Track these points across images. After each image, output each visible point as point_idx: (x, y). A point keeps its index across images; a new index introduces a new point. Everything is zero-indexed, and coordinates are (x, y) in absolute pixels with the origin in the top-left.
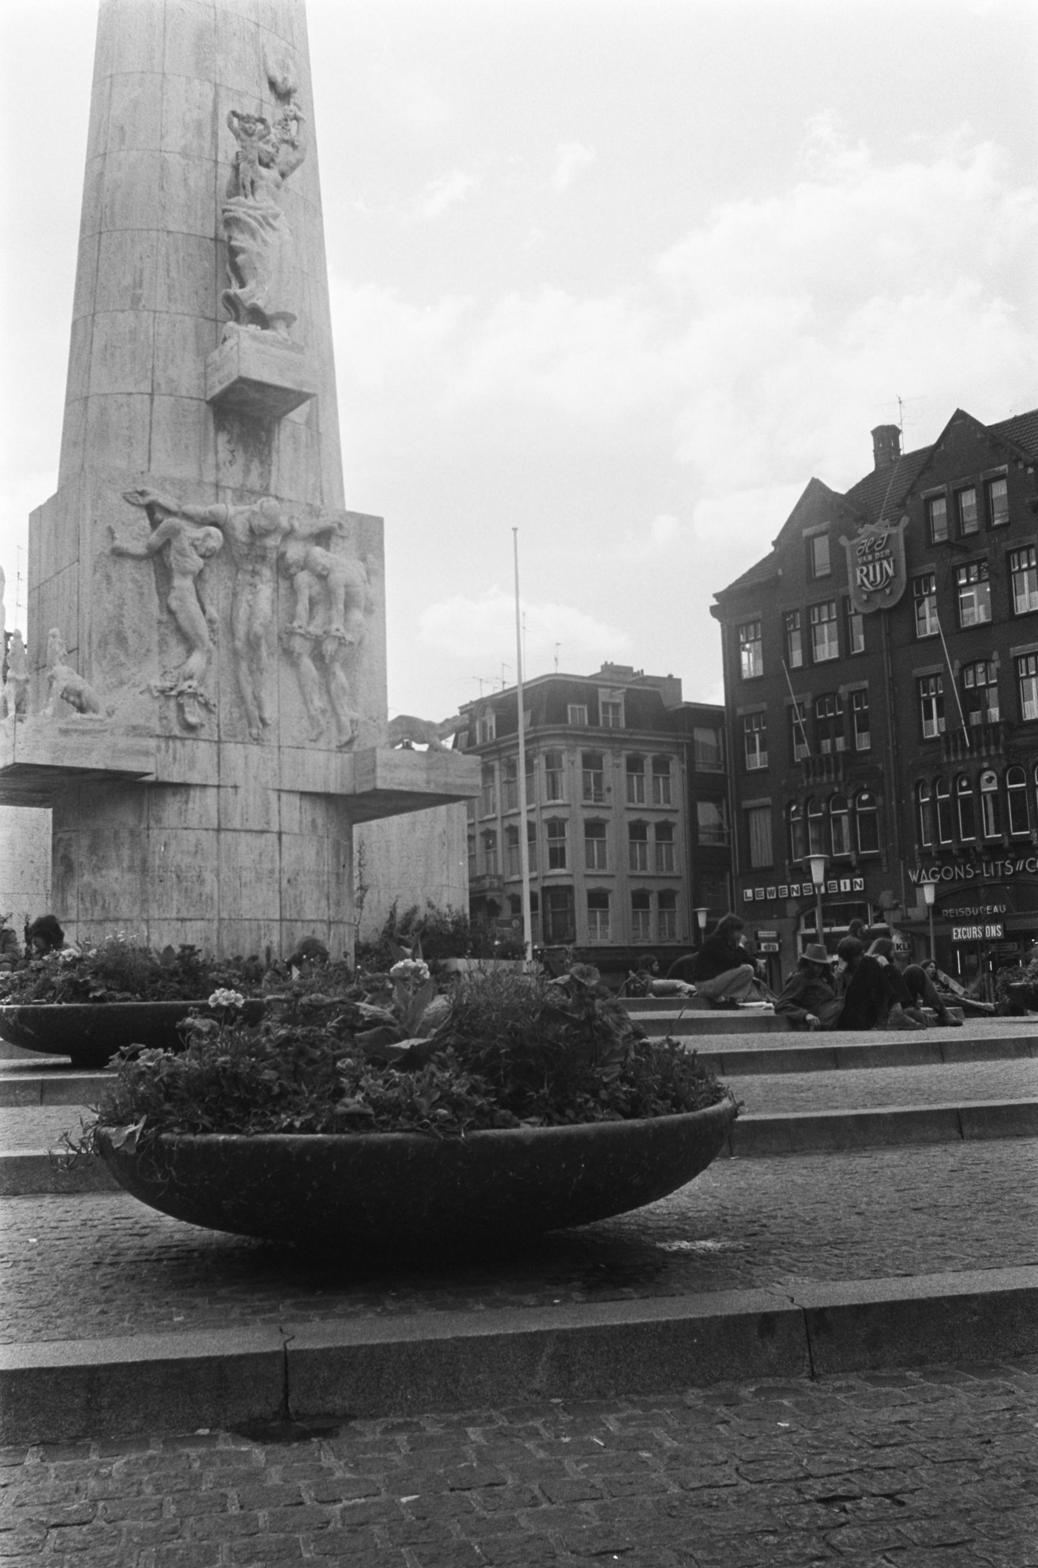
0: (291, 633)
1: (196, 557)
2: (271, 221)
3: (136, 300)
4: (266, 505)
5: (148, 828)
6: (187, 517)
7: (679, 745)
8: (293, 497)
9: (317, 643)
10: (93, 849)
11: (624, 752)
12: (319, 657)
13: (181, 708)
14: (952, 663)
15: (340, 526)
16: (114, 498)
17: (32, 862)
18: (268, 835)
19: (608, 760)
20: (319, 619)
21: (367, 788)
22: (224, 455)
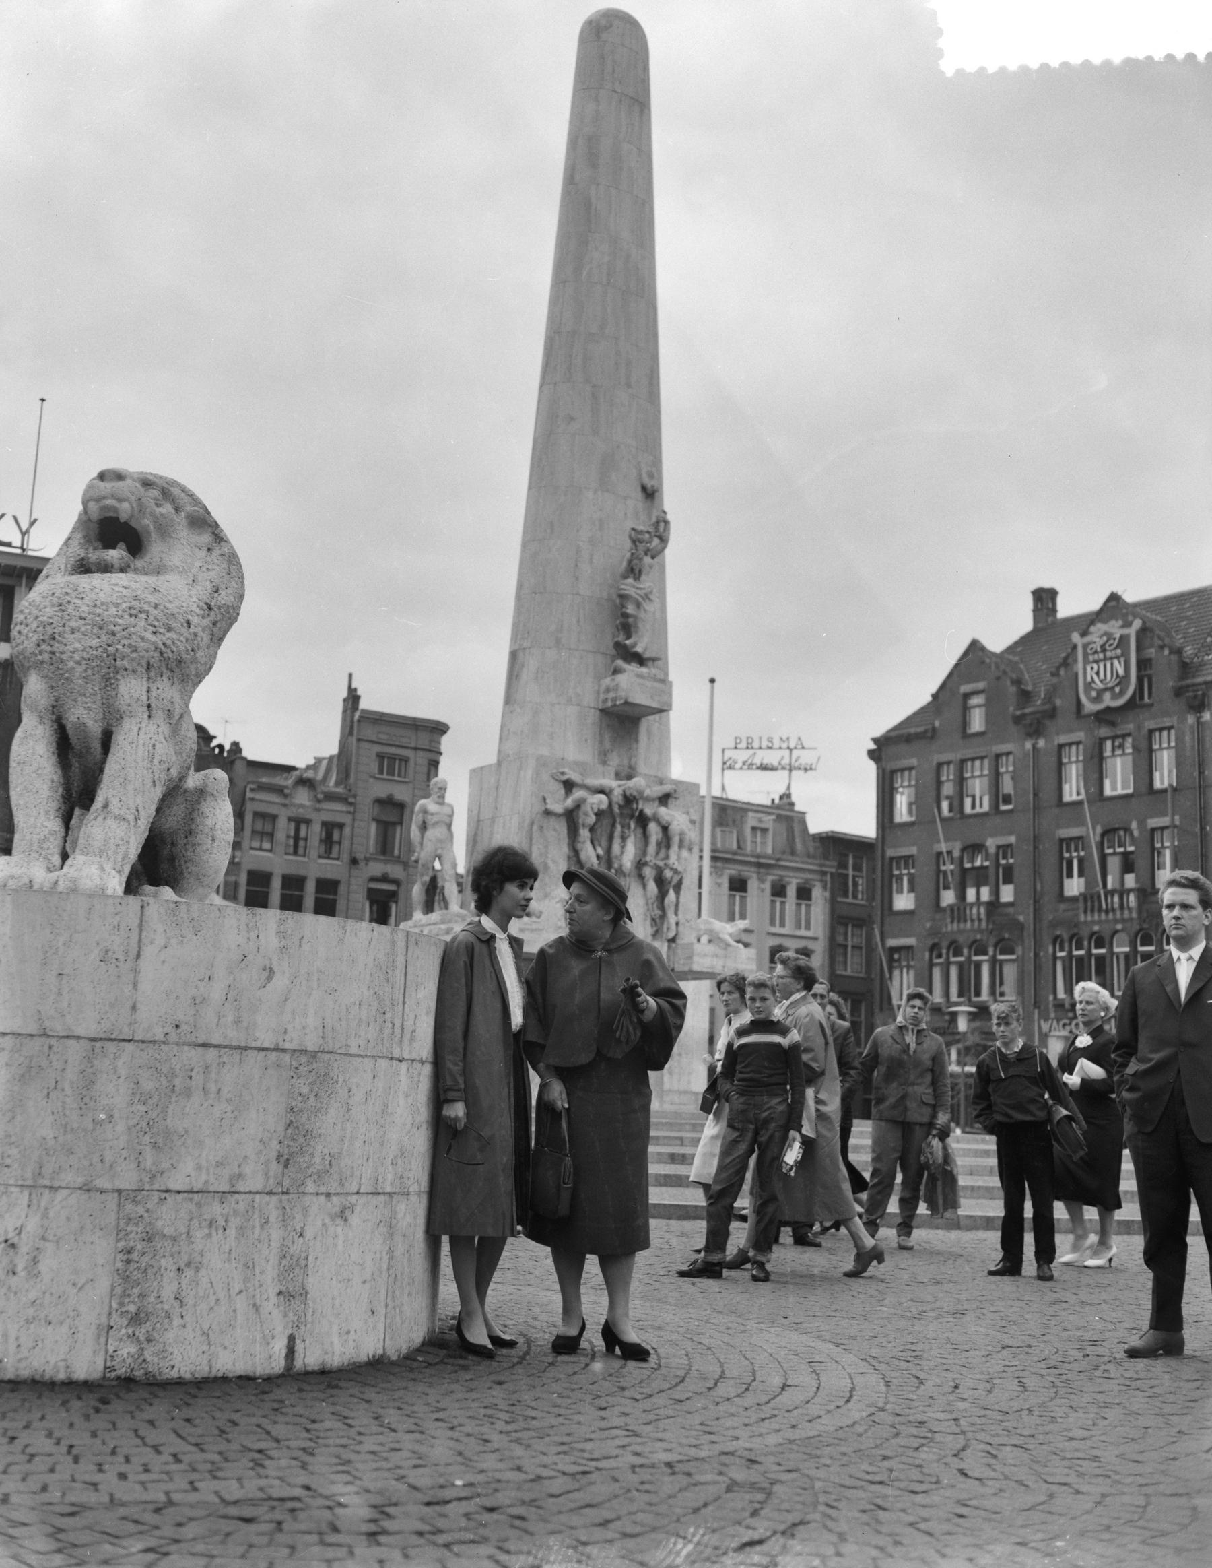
0: (646, 864)
3: (558, 641)
7: (824, 873)
11: (770, 878)
12: (660, 881)
14: (1094, 829)
16: (546, 776)
19: (753, 885)
20: (662, 855)
21: (686, 969)
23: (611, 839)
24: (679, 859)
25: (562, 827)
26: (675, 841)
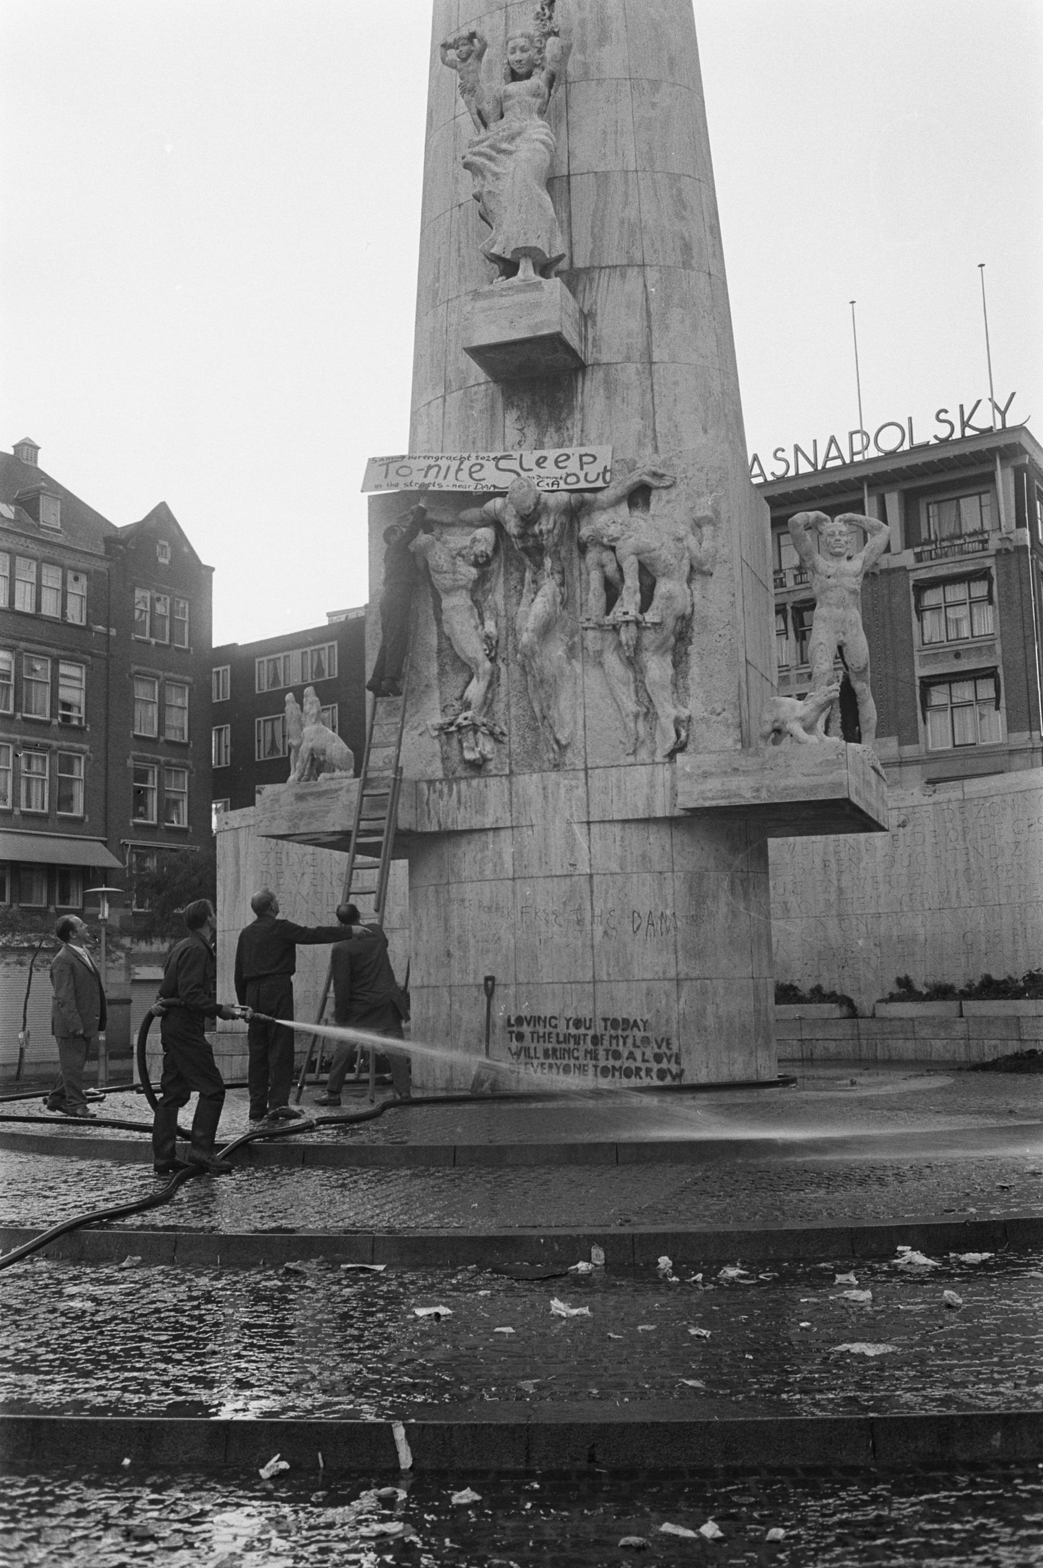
2: (504, 146)
5: (448, 883)
13: (460, 742)
15: (655, 474)
18: (576, 878)
22: (512, 434)
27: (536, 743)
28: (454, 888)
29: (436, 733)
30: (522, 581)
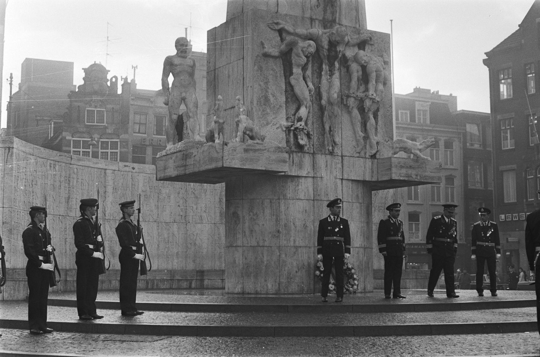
0: (348, 96)
1: (304, 57)
4: (339, 30)
5: (279, 199)
6: (299, 36)
8: (347, 24)
9: (361, 101)
10: (251, 209)
12: (362, 110)
15: (371, 38)
17: (179, 206)
21: (385, 178)
23: (320, 76)
24: (376, 91)
25: (278, 67)
26: (374, 75)
27: (324, 142)
28: (282, 202)
29: (284, 129)
30: (320, 69)
